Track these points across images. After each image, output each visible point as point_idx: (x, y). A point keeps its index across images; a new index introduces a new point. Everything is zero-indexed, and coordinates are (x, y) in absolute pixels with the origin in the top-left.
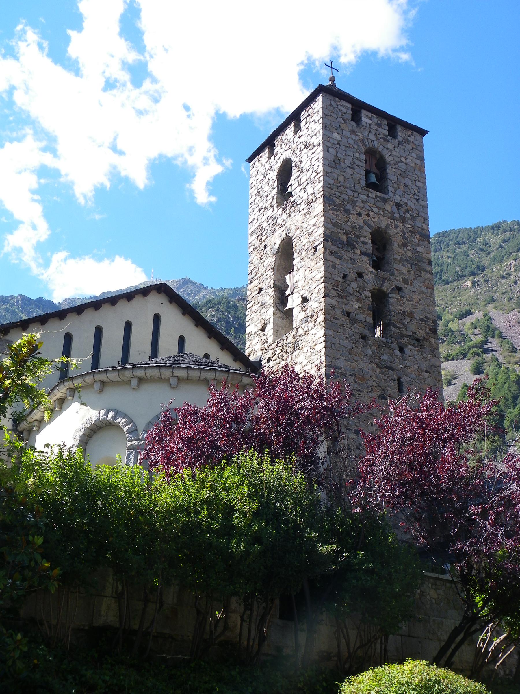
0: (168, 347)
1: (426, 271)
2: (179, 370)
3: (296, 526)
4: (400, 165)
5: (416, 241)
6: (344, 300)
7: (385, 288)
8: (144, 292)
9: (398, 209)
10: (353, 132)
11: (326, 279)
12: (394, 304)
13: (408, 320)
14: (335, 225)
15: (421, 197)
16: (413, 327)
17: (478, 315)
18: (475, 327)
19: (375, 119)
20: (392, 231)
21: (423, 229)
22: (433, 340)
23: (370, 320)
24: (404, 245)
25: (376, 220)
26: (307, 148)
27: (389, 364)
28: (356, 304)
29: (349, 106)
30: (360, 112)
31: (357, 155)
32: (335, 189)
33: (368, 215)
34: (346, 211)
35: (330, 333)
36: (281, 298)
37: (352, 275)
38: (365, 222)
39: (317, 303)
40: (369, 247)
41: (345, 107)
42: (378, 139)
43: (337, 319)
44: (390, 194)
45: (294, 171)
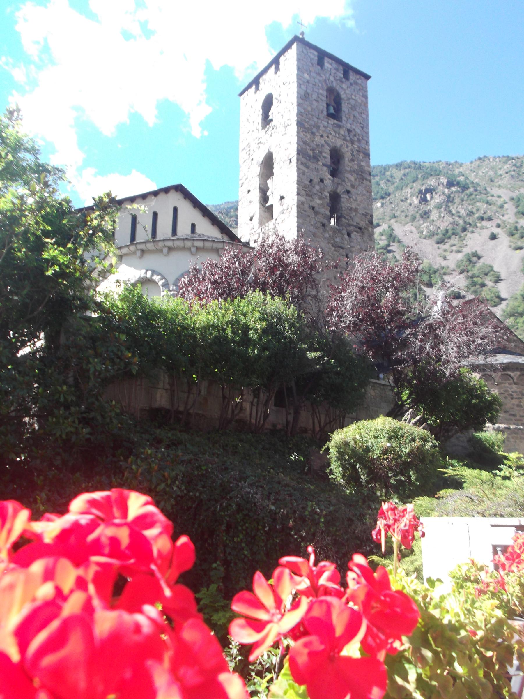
0: (184, 230)
1: (367, 180)
2: (194, 244)
3: (291, 341)
4: (351, 101)
5: (361, 157)
6: (310, 198)
7: (338, 191)
8: (166, 190)
9: (349, 133)
10: (319, 74)
11: (299, 182)
12: (345, 202)
13: (354, 214)
14: (305, 143)
15: (365, 126)
16: (358, 220)
17: (384, 227)
18: (382, 235)
19: (335, 65)
20: (344, 150)
21: (366, 149)
22: (370, 229)
23: (328, 213)
24: (352, 160)
25: (333, 141)
26: (285, 86)
27: (340, 245)
28: (318, 201)
29: (316, 53)
30: (323, 59)
31: (321, 91)
32: (305, 115)
33: (328, 137)
34: (313, 133)
35: (301, 221)
36: (264, 198)
37: (316, 180)
38: (326, 142)
39: (292, 199)
40: (328, 161)
41: (313, 54)
42: (336, 80)
43: (305, 211)
44: (344, 122)
45: (274, 101)
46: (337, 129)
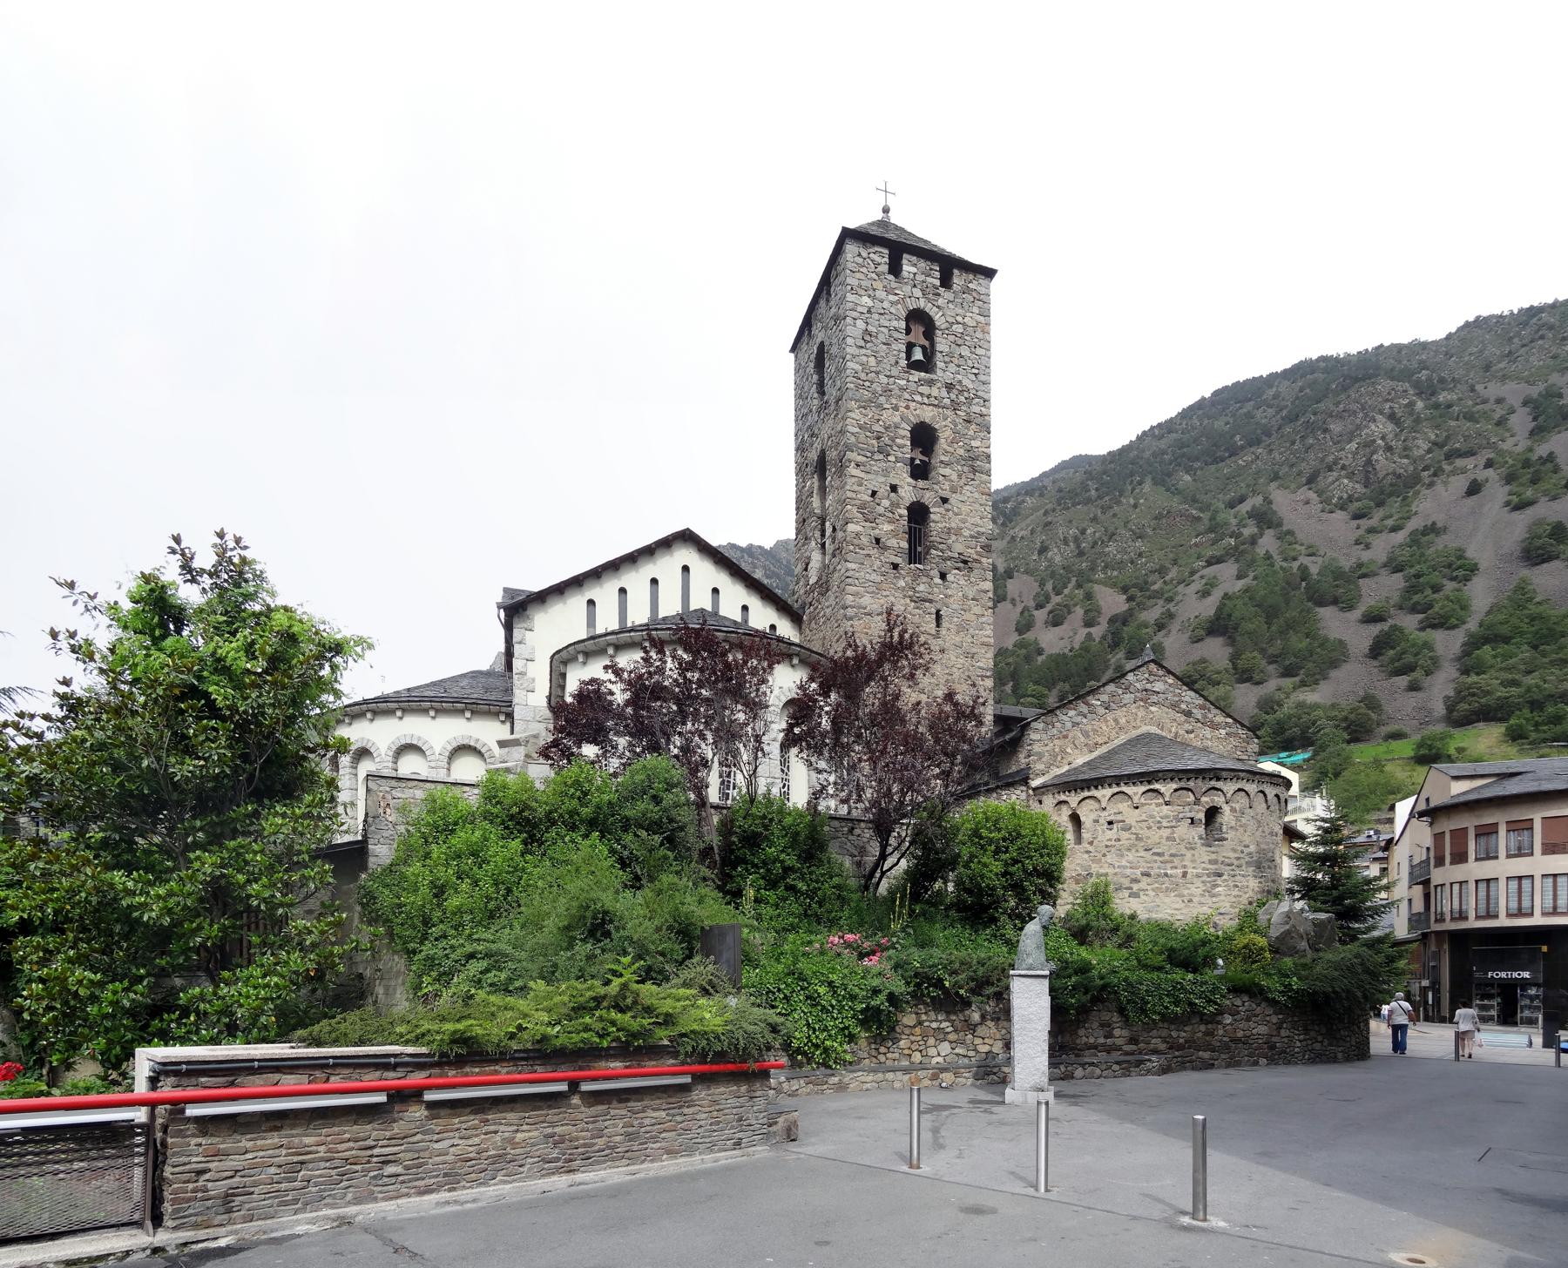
15: (981, 372)
28: (887, 527)
33: (907, 407)
37: (883, 490)
44: (939, 372)
46: (925, 389)
